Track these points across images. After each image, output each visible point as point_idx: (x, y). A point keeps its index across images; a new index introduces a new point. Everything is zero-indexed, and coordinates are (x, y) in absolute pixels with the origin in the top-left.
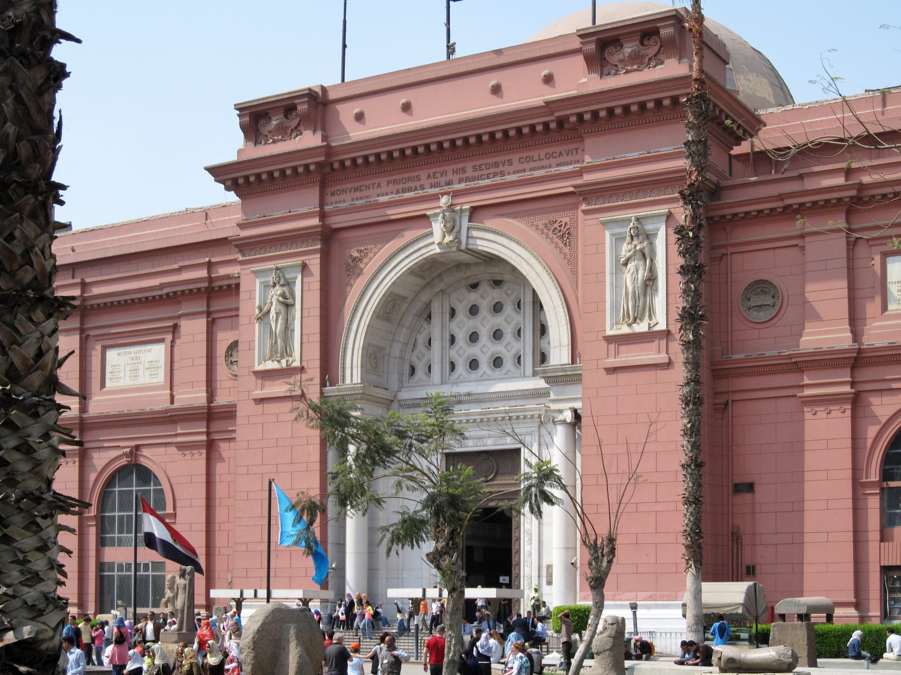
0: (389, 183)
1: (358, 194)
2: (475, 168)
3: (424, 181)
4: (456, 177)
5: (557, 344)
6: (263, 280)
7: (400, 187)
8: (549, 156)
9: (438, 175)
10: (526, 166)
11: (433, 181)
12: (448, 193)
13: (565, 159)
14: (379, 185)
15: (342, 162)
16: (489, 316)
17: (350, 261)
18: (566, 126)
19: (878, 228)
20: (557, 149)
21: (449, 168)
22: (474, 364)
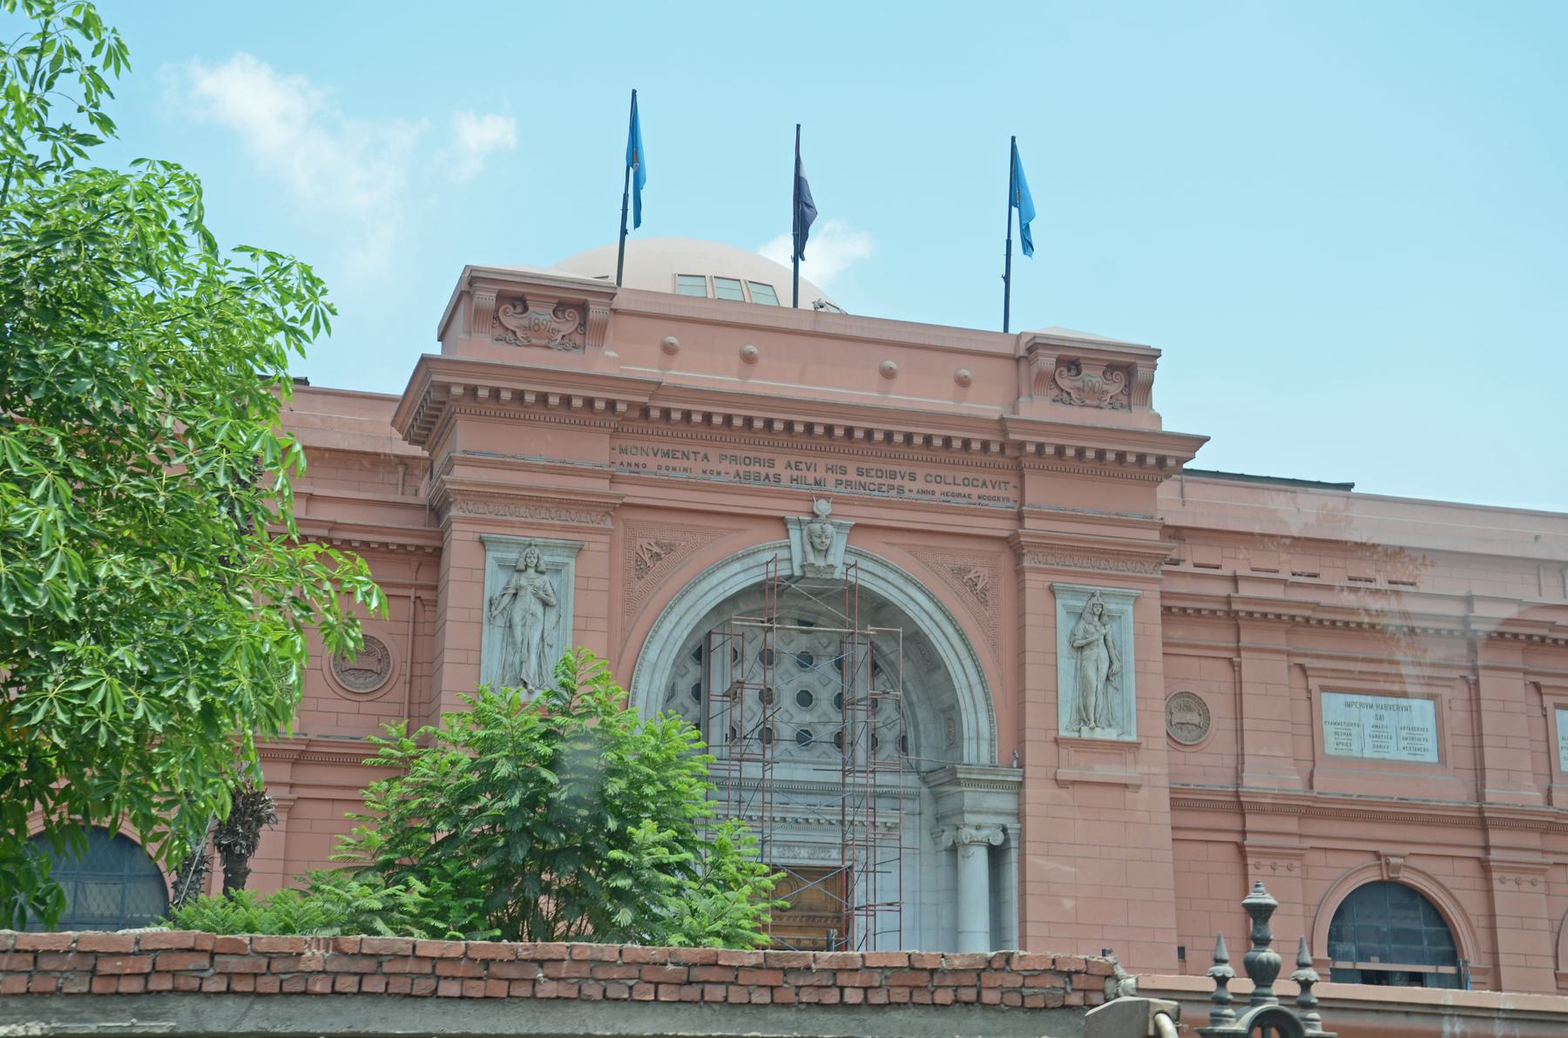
0: (723, 457)
1: (671, 462)
2: (860, 472)
3: (779, 468)
4: (831, 478)
5: (973, 734)
6: (499, 555)
7: (742, 469)
8: (967, 482)
9: (802, 466)
10: (933, 487)
11: (795, 474)
12: (827, 498)
13: (989, 491)
14: (706, 457)
15: (666, 413)
16: (794, 670)
17: (646, 557)
18: (1008, 452)
19: (1380, 661)
20: (982, 477)
21: (822, 464)
22: (767, 736)
